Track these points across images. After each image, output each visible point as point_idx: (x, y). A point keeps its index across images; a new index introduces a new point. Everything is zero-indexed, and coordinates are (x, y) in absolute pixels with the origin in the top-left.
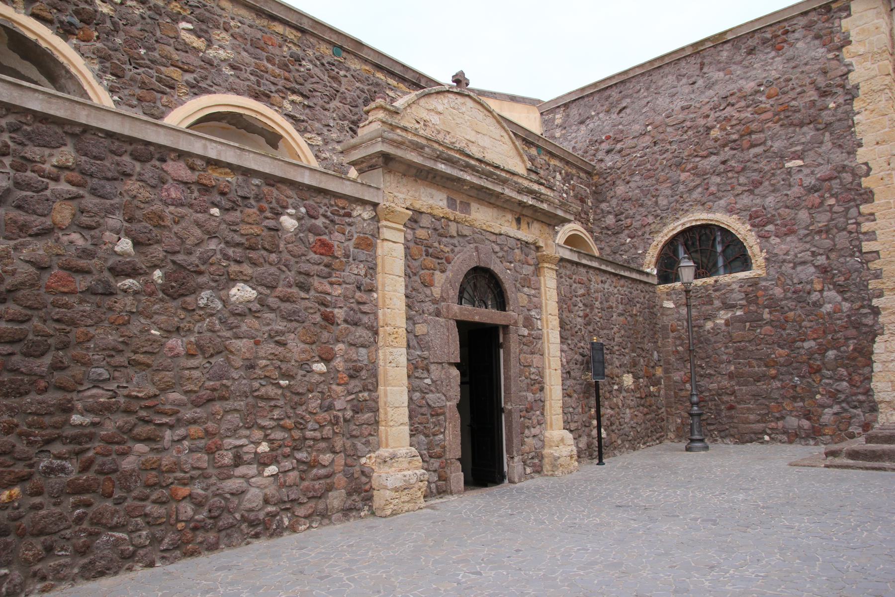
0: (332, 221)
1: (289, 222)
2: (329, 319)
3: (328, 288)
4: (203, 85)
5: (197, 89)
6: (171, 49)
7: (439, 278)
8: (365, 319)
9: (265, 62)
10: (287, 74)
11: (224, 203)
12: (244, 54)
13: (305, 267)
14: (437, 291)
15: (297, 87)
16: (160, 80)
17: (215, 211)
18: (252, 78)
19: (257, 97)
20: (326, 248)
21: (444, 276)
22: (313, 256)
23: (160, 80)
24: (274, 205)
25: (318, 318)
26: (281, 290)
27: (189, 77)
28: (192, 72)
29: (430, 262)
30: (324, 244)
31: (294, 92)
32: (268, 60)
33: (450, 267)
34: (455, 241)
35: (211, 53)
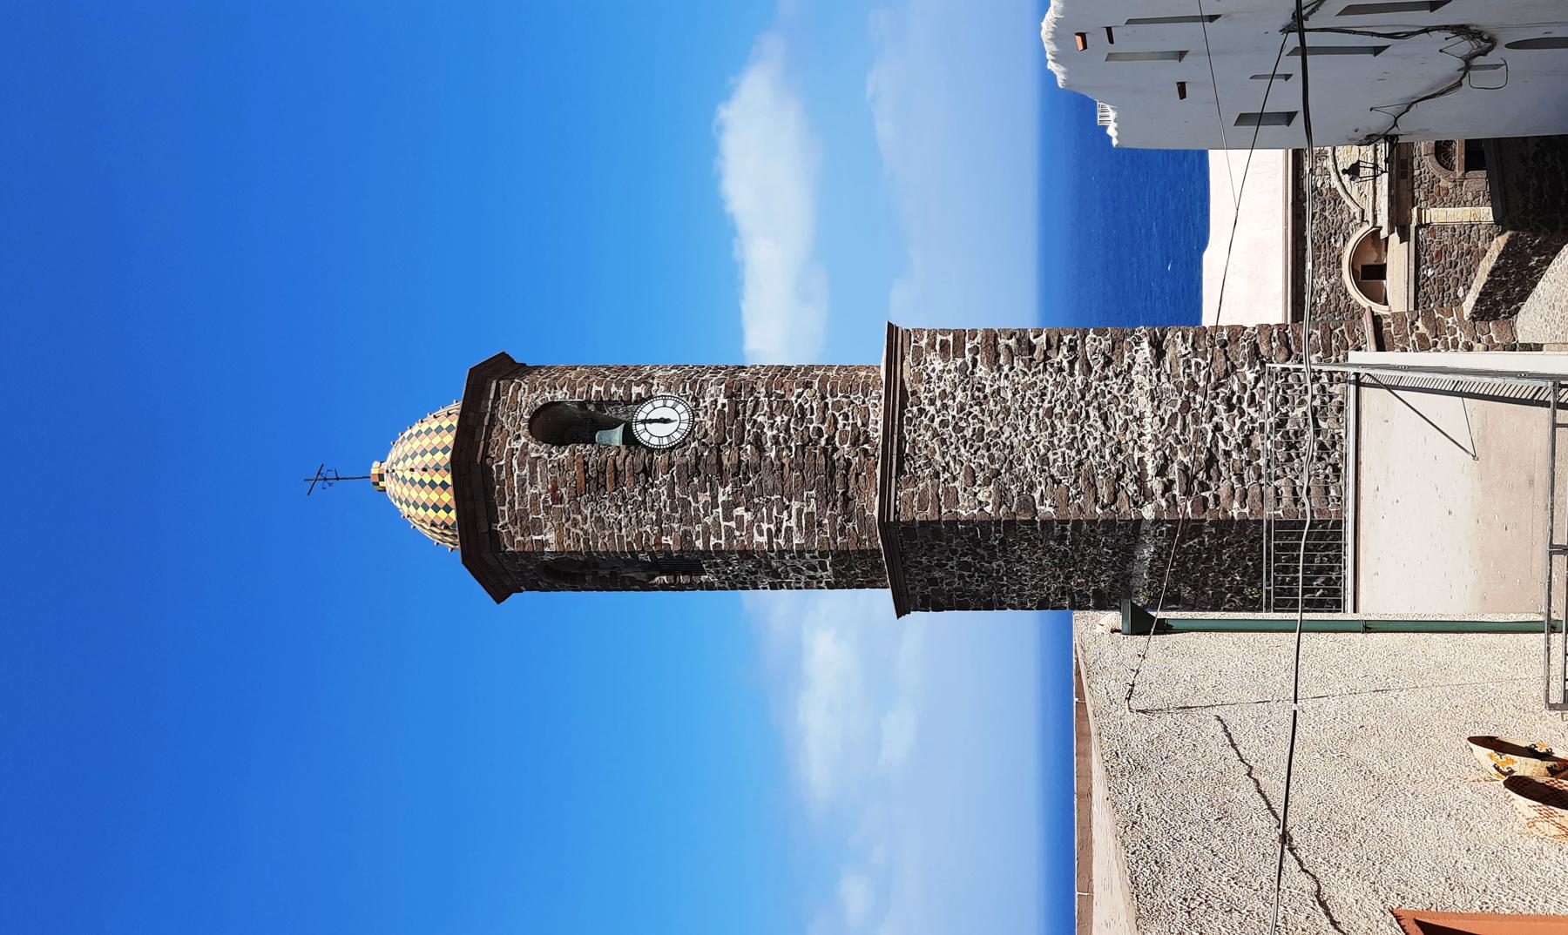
0: (1427, 250)
1: (1430, 272)
2: (1469, 252)
3: (1455, 252)
4: (1344, 292)
5: (1346, 294)
6: (1332, 307)
7: (1443, 183)
8: (1467, 232)
9: (1321, 259)
10: (1323, 247)
11: (1428, 302)
12: (1321, 271)
13: (1448, 265)
14: (1450, 185)
15: (1327, 241)
16: (1348, 311)
17: (1432, 305)
18: (1332, 266)
19: (1340, 264)
20: (1439, 254)
21: (1442, 180)
22: (1443, 261)
23: (1348, 311)
24: (1424, 280)
25: (1468, 257)
26: (1458, 275)
27: (1342, 298)
28: (1339, 297)
29: (1435, 190)
30: (1437, 256)
31: (1330, 242)
32: (1319, 258)
33: (1437, 176)
34: (1423, 170)
35: (1328, 289)
